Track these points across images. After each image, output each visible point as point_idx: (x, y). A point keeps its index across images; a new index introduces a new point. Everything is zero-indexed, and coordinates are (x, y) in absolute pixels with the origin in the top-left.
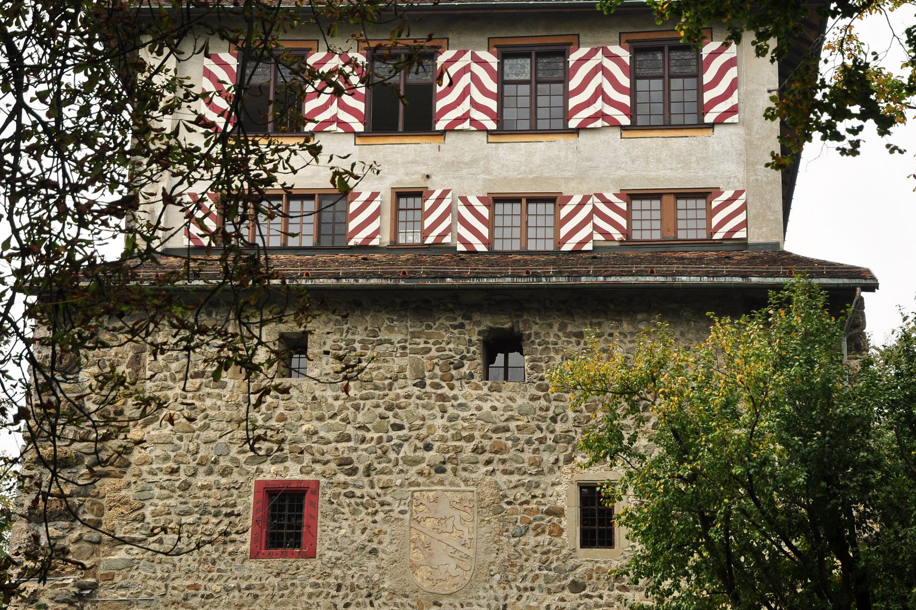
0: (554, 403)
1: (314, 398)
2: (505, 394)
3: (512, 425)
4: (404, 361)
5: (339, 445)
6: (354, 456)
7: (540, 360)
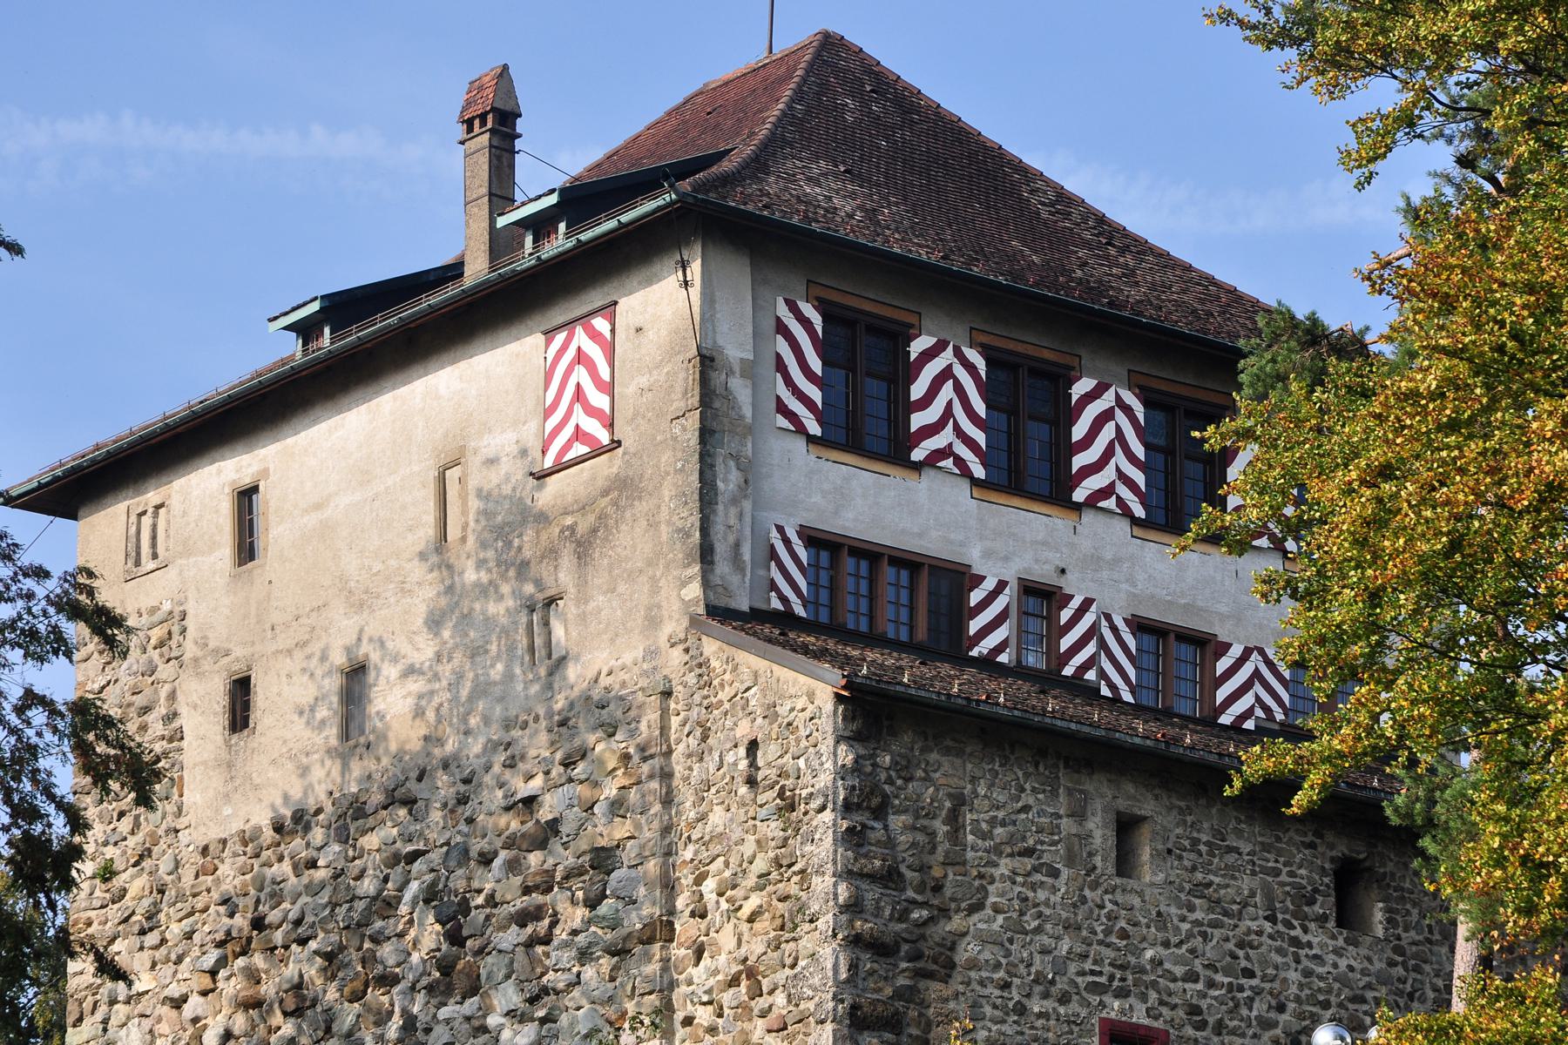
0: (1413, 975)
1: (1159, 914)
2: (1364, 951)
3: (1370, 995)
4: (1255, 883)
5: (1188, 986)
6: (1204, 1004)
7: (1397, 911)
